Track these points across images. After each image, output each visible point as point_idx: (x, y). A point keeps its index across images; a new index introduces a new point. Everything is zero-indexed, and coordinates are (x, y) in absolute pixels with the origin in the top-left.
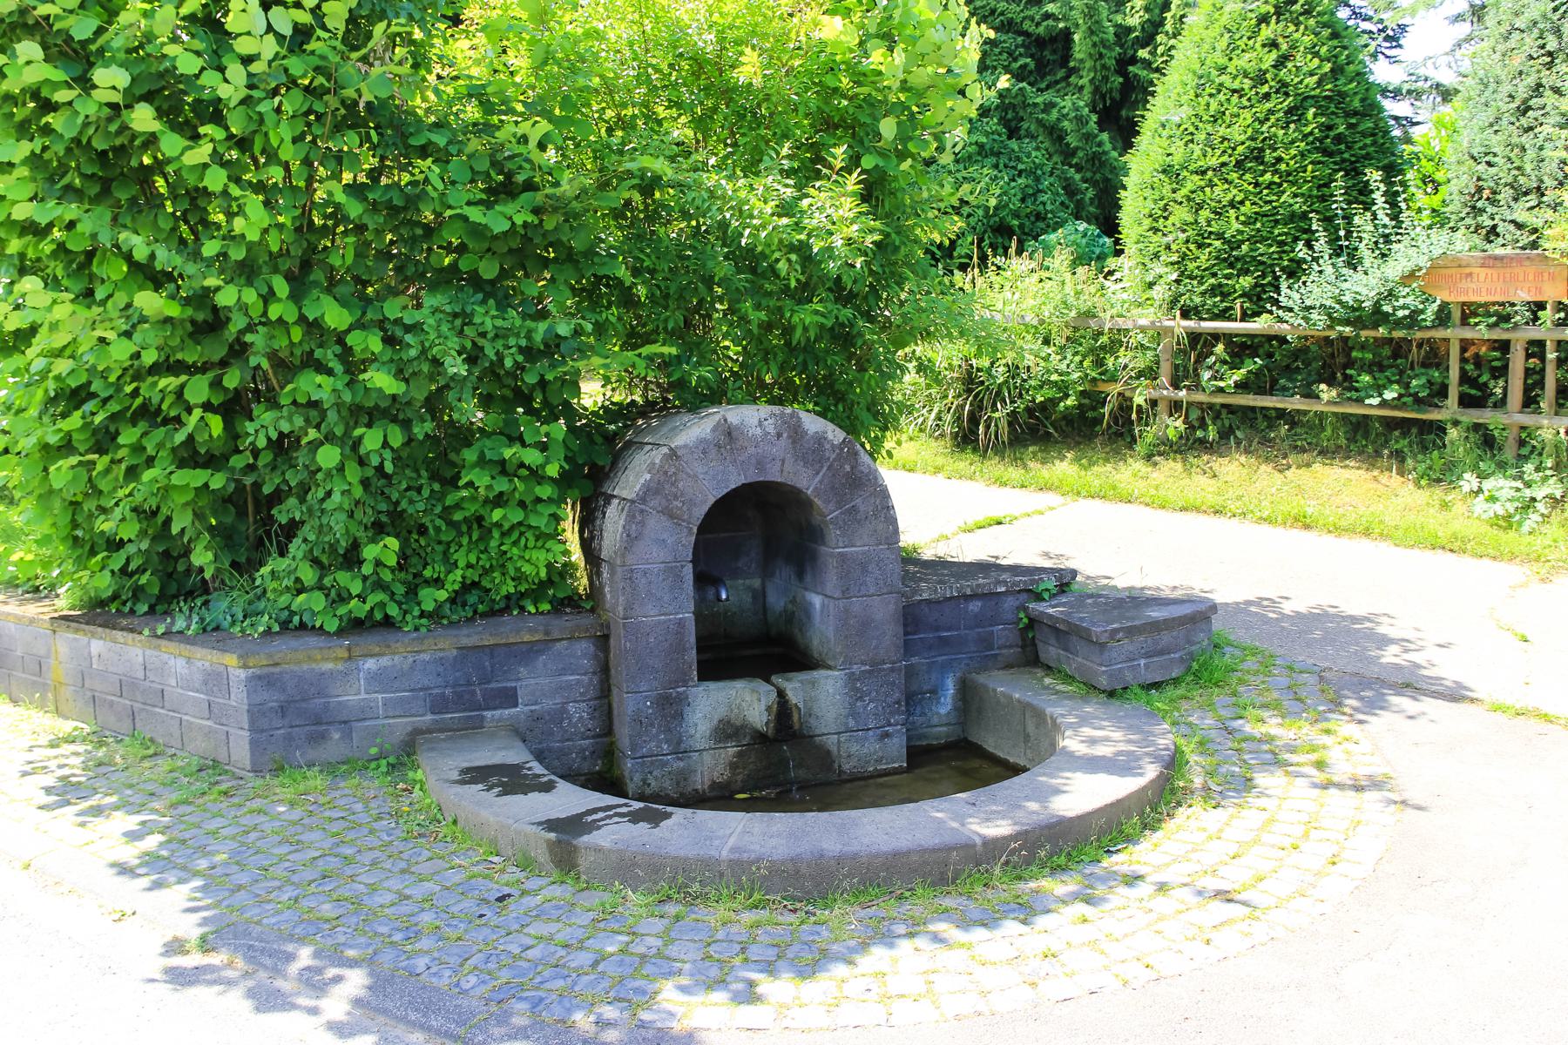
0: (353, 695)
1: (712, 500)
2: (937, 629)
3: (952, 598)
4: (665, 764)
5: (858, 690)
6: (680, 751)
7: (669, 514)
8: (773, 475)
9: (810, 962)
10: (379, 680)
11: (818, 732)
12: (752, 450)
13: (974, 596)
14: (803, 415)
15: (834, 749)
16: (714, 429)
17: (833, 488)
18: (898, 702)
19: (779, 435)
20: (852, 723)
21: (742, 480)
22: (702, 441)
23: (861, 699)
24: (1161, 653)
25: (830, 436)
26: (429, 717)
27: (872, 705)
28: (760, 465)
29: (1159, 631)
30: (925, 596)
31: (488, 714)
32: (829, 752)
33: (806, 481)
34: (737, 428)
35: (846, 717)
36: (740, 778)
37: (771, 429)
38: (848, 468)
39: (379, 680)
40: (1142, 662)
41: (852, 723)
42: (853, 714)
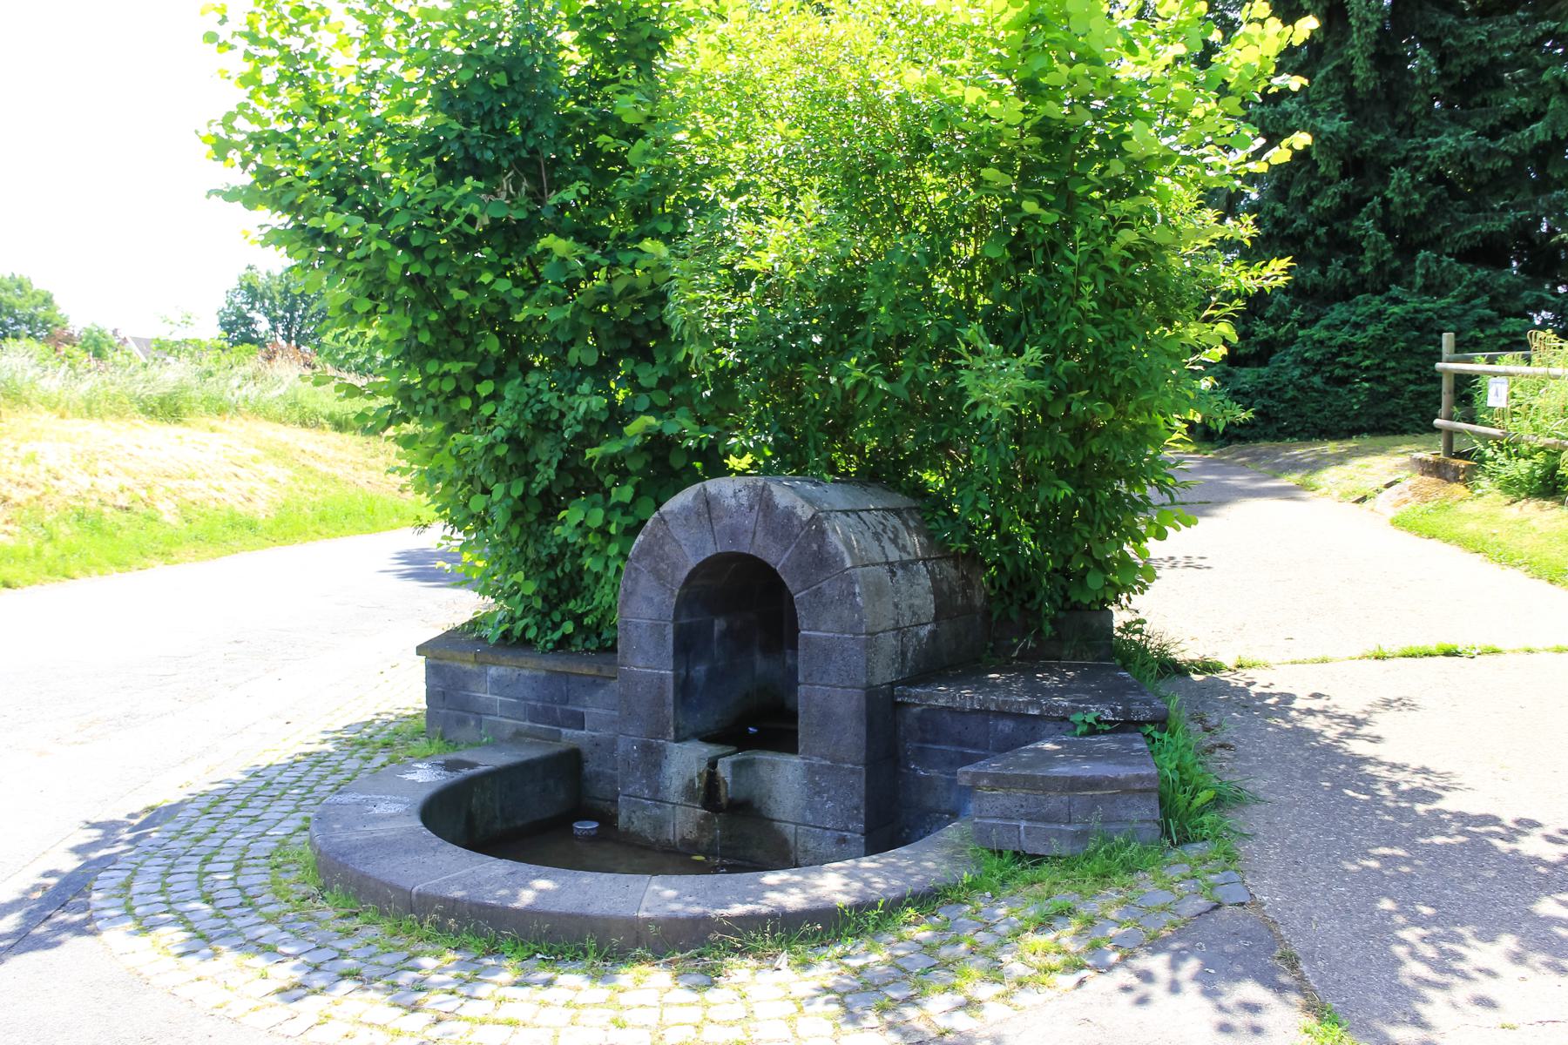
0: (483, 694)
1: (692, 563)
2: (961, 743)
3: (974, 711)
4: (645, 808)
5: (817, 784)
6: (660, 801)
7: (657, 574)
8: (746, 548)
9: (327, 969)
10: (500, 685)
11: (776, 816)
12: (726, 521)
13: (1001, 714)
14: (774, 487)
15: (792, 840)
16: (696, 497)
17: (799, 566)
18: (856, 808)
19: (751, 508)
20: (809, 817)
21: (710, 551)
22: (684, 508)
23: (819, 793)
24: (1047, 819)
25: (799, 511)
26: (527, 723)
27: (830, 804)
28: (734, 534)
29: (1045, 790)
30: (942, 702)
31: (564, 731)
32: (786, 841)
33: (777, 557)
34: (715, 498)
35: (804, 809)
36: (705, 840)
37: (744, 501)
38: (815, 547)
39: (500, 685)
40: (1023, 824)
41: (809, 817)
42: (810, 807)
